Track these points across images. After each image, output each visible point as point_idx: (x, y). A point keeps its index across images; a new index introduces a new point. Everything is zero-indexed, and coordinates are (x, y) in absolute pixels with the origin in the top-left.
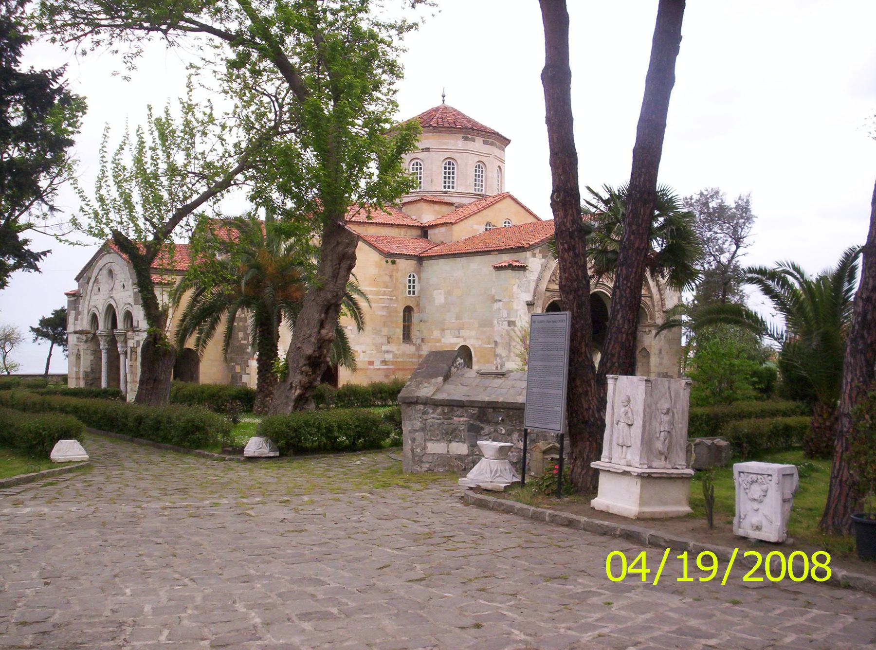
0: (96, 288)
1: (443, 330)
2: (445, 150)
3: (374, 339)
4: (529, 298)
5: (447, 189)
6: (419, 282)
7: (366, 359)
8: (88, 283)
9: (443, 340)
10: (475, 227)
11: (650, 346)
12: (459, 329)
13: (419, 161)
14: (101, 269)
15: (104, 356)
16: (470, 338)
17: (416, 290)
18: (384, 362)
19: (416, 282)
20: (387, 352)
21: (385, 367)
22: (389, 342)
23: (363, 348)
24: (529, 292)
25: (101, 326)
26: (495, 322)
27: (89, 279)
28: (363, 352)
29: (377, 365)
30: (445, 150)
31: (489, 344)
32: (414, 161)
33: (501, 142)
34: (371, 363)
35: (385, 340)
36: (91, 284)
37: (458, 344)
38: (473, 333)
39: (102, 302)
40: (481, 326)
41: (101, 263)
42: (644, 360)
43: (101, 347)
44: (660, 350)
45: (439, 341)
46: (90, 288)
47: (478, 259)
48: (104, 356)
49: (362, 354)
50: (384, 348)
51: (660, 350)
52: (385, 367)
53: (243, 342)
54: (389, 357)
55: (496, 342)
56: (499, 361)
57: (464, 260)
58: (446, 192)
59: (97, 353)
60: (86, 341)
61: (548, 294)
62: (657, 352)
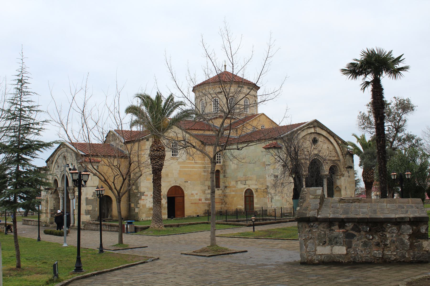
0: (56, 166)
1: (237, 182)
8: (52, 163)
11: (341, 185)
12: (245, 181)
14: (59, 156)
15: (61, 201)
16: (252, 185)
23: (196, 192)
25: (59, 185)
26: (267, 176)
27: (53, 161)
28: (196, 194)
33: (256, 88)
34: (200, 200)
36: (54, 164)
39: (60, 173)
41: (59, 153)
42: (338, 193)
43: (60, 196)
44: (346, 187)
45: (235, 187)
46: (53, 166)
48: (61, 201)
49: (196, 195)
51: (346, 187)
53: (135, 191)
55: (268, 186)
56: (270, 196)
59: (57, 199)
60: (51, 194)
62: (344, 188)
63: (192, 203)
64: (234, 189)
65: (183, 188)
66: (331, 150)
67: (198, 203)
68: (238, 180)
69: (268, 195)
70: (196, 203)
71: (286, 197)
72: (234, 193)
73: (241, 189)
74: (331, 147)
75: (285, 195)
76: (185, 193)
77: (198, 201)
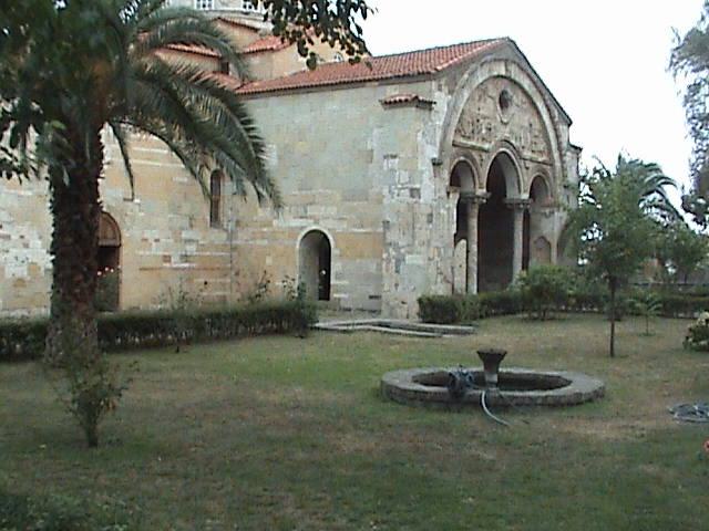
3: (171, 219)
4: (436, 156)
5: (248, 10)
7: (161, 253)
9: (275, 222)
18: (185, 258)
20: (189, 241)
21: (186, 265)
22: (191, 226)
24: (435, 144)
28: (157, 240)
29: (176, 262)
31: (362, 227)
34: (167, 259)
35: (186, 222)
37: (302, 228)
38: (333, 211)
40: (346, 199)
47: (339, 95)
49: (154, 244)
50: (185, 235)
52: (186, 265)
54: (191, 249)
57: (314, 97)
58: (247, 14)
61: (454, 150)
63: (141, 269)
64: (265, 230)
65: (117, 219)
66: (537, 133)
67: (160, 268)
69: (387, 251)
70: (152, 269)
71: (437, 259)
72: (265, 242)
73: (293, 232)
74: (537, 126)
75: (436, 253)
76: (125, 234)
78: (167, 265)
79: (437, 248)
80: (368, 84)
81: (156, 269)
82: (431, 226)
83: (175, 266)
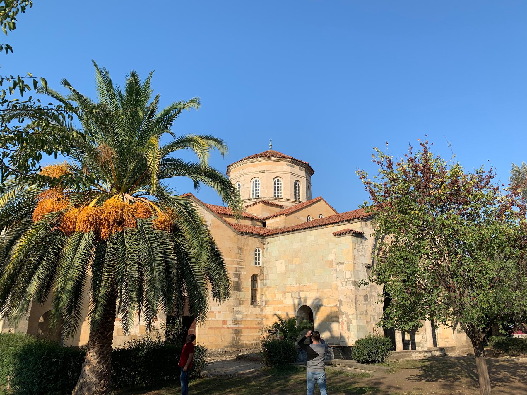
1: (285, 293)
2: (275, 172)
6: (263, 256)
7: (221, 319)
10: (300, 218)
13: (258, 179)
17: (261, 261)
19: (261, 255)
21: (237, 326)
28: (219, 312)
29: (230, 324)
30: (275, 172)
32: (254, 179)
34: (225, 322)
49: (217, 315)
52: (237, 326)
56: (345, 319)
67: (221, 328)
68: (287, 290)
75: (372, 318)
77: (221, 325)
78: (225, 326)
79: (372, 315)
80: (327, 226)
81: (218, 328)
82: (367, 303)
83: (229, 326)
